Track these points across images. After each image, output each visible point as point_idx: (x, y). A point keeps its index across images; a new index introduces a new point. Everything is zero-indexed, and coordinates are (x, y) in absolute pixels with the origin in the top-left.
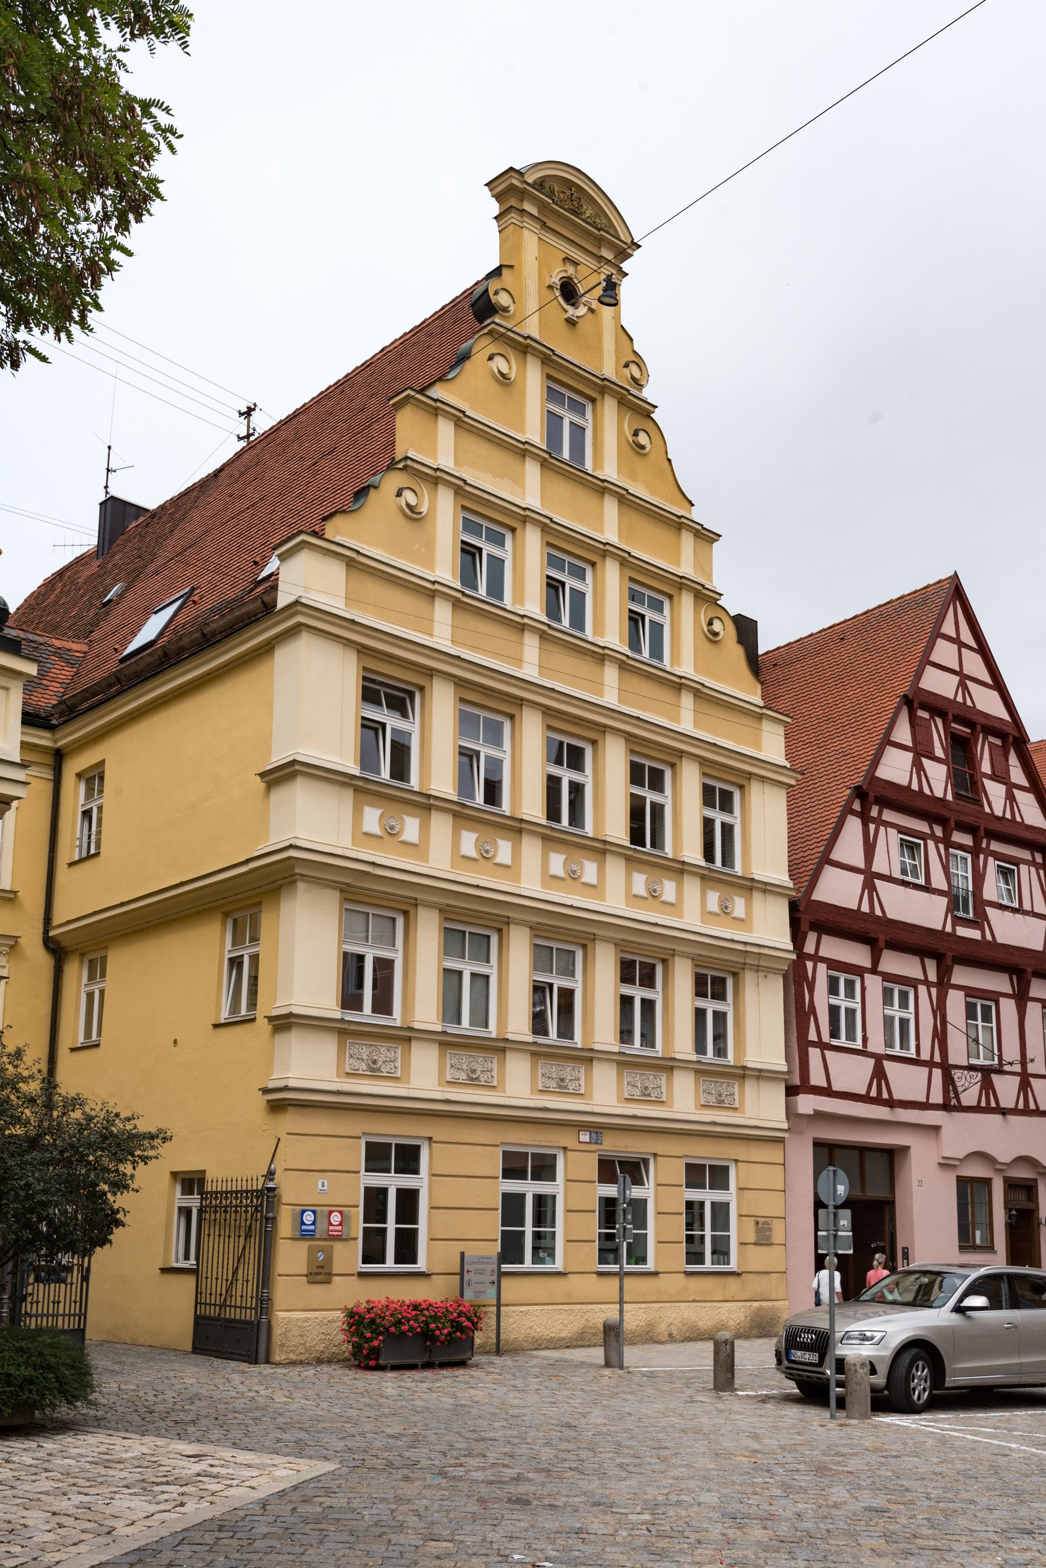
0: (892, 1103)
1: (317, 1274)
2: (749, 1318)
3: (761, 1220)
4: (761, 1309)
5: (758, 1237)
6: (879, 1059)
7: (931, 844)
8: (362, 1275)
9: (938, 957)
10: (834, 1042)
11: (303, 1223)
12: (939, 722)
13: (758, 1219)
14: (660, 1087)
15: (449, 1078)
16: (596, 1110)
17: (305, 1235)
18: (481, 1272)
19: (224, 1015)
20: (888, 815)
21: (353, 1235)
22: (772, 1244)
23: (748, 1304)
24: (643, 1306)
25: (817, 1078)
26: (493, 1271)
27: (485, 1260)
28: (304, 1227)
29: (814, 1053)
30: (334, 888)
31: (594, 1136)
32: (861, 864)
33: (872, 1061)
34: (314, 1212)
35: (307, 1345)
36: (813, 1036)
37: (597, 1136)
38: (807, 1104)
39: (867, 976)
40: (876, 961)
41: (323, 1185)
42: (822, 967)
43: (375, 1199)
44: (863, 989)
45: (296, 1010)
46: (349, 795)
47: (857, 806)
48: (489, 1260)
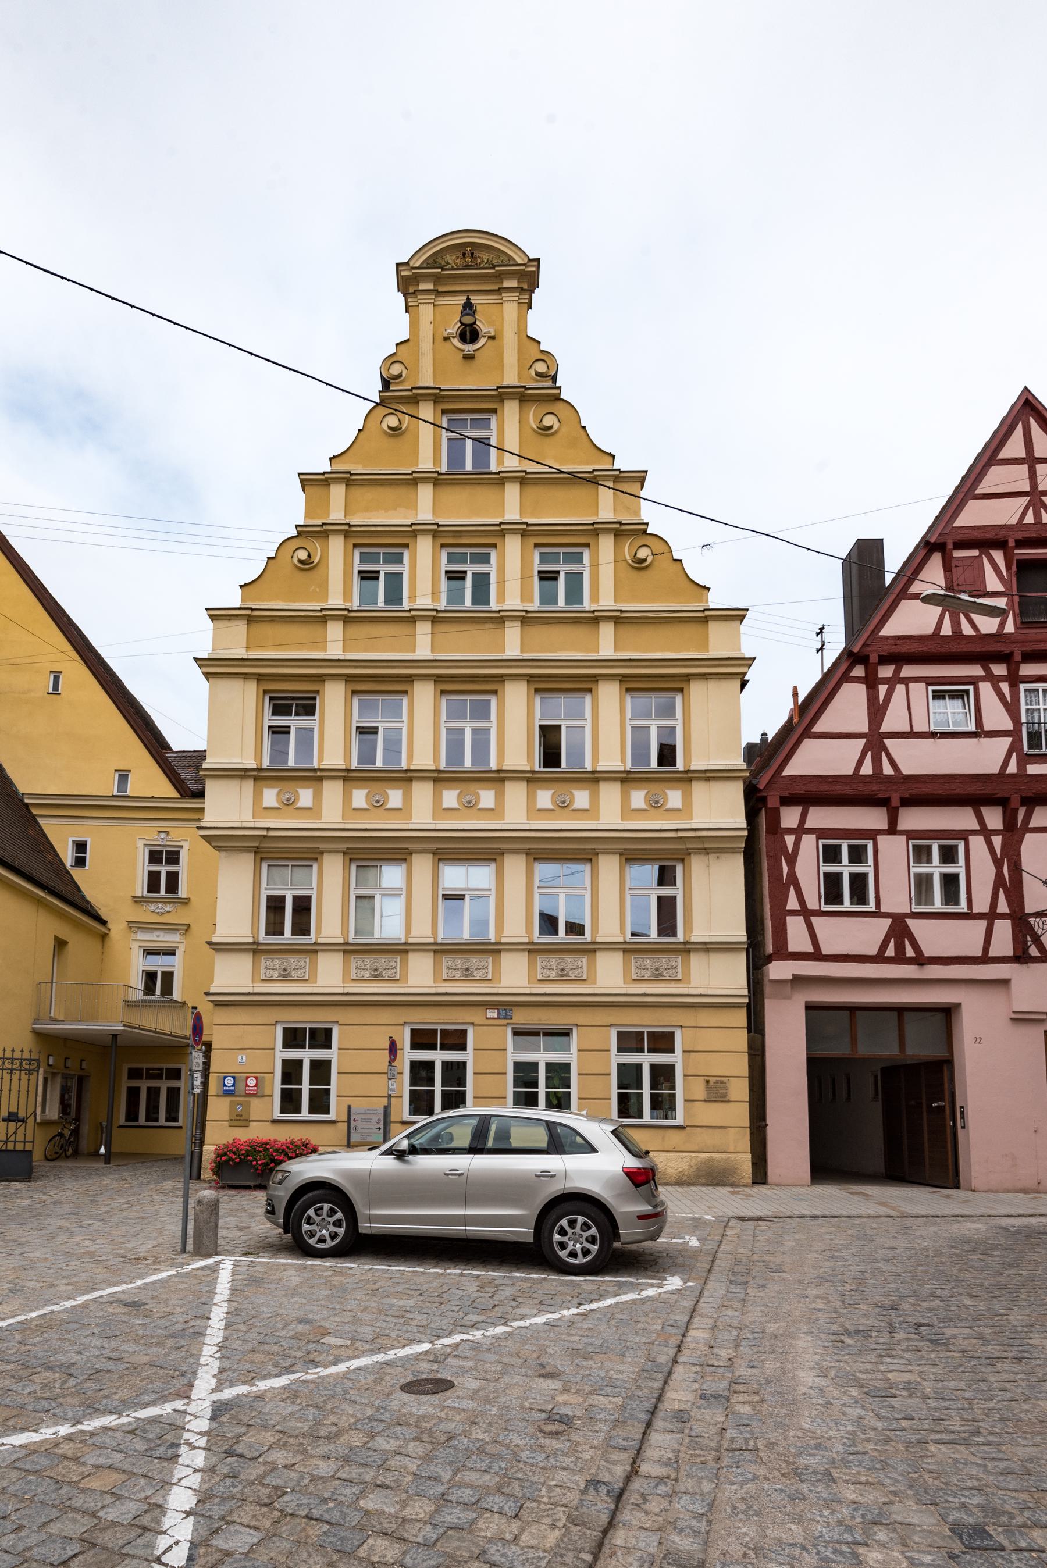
2: (694, 1168)
5: (708, 1095)
8: (275, 1122)
11: (225, 1085)
14: (581, 967)
16: (501, 991)
17: (228, 1094)
21: (267, 1092)
22: (729, 1101)
23: (694, 1155)
28: (225, 1088)
37: (506, 1013)
41: (242, 1059)
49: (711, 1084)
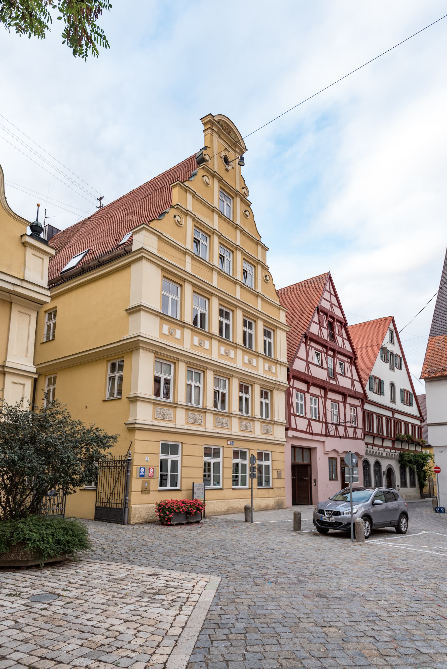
0: (312, 434)
3: (278, 471)
4: (279, 500)
6: (309, 420)
7: (323, 354)
8: (159, 491)
9: (325, 389)
10: (298, 414)
11: (140, 472)
12: (325, 316)
17: (142, 476)
18: (199, 489)
19: (107, 397)
20: (312, 344)
24: (246, 499)
25: (293, 426)
28: (141, 474)
29: (292, 417)
30: (152, 352)
32: (305, 359)
33: (308, 421)
34: (144, 468)
36: (292, 412)
38: (291, 433)
39: (306, 394)
40: (308, 389)
42: (294, 390)
43: (163, 464)
44: (305, 398)
45: (139, 395)
46: (158, 319)
47: (304, 340)
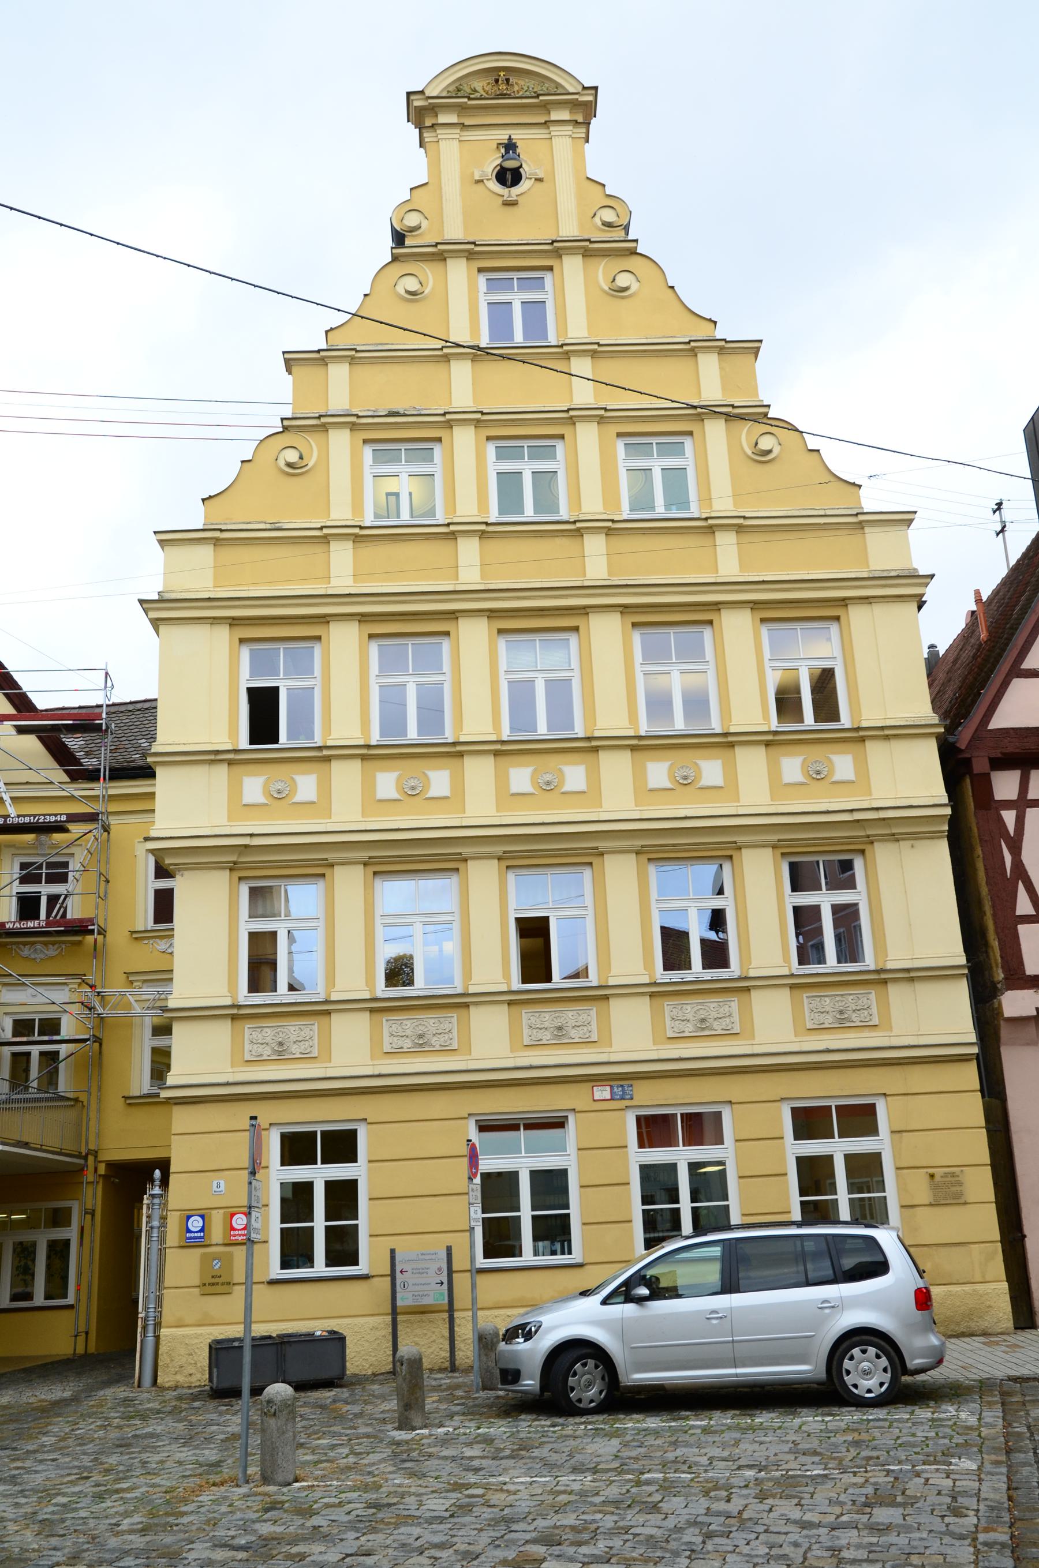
1: (213, 1284)
13: (931, 1171)
15: (387, 1048)
16: (614, 1058)
18: (422, 1272)
22: (965, 1203)
26: (440, 1269)
27: (427, 1257)
31: (618, 1091)
35: (199, 1365)
37: (623, 1090)
41: (218, 1186)
48: (433, 1257)
49: (937, 1178)
